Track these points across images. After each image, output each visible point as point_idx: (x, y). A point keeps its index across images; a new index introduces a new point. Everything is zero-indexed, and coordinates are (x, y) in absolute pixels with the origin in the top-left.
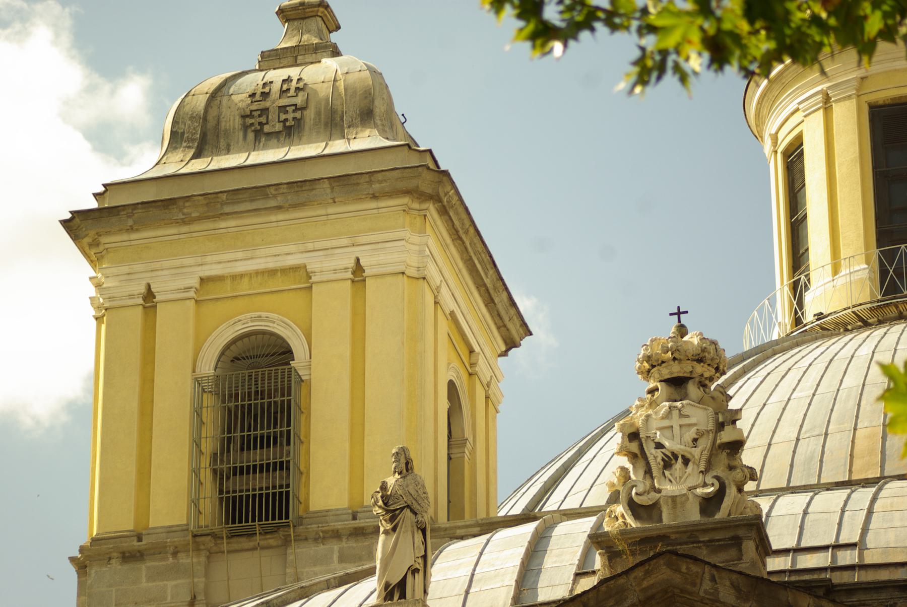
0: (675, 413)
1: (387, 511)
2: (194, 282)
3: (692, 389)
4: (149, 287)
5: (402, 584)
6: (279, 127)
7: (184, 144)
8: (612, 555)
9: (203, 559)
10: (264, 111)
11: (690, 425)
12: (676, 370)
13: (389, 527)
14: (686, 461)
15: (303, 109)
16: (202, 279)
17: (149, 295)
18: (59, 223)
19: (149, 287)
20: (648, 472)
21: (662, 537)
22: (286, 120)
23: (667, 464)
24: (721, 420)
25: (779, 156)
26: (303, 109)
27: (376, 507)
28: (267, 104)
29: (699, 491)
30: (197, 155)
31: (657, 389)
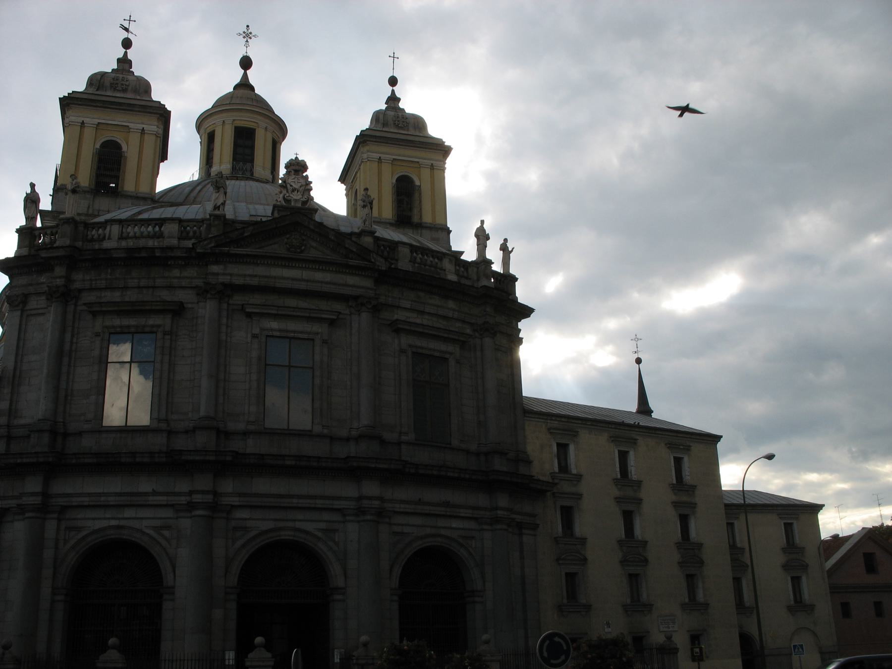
0: (296, 179)
1: (216, 186)
2: (97, 123)
3: (300, 173)
4: (83, 121)
5: (219, 206)
6: (121, 89)
7: (94, 87)
8: (279, 211)
9: (92, 196)
10: (117, 84)
11: (299, 182)
12: (297, 168)
13: (217, 191)
14: (298, 192)
15: (128, 86)
16: (99, 123)
17: (83, 123)
18: (58, 99)
19: (83, 121)
20: (287, 192)
21: (293, 208)
22: (123, 88)
23: (293, 190)
24: (307, 183)
25: (207, 134)
26: (128, 86)
27: (228, 182)
28: (117, 82)
29: (302, 199)
30: (97, 90)
31: (291, 171)
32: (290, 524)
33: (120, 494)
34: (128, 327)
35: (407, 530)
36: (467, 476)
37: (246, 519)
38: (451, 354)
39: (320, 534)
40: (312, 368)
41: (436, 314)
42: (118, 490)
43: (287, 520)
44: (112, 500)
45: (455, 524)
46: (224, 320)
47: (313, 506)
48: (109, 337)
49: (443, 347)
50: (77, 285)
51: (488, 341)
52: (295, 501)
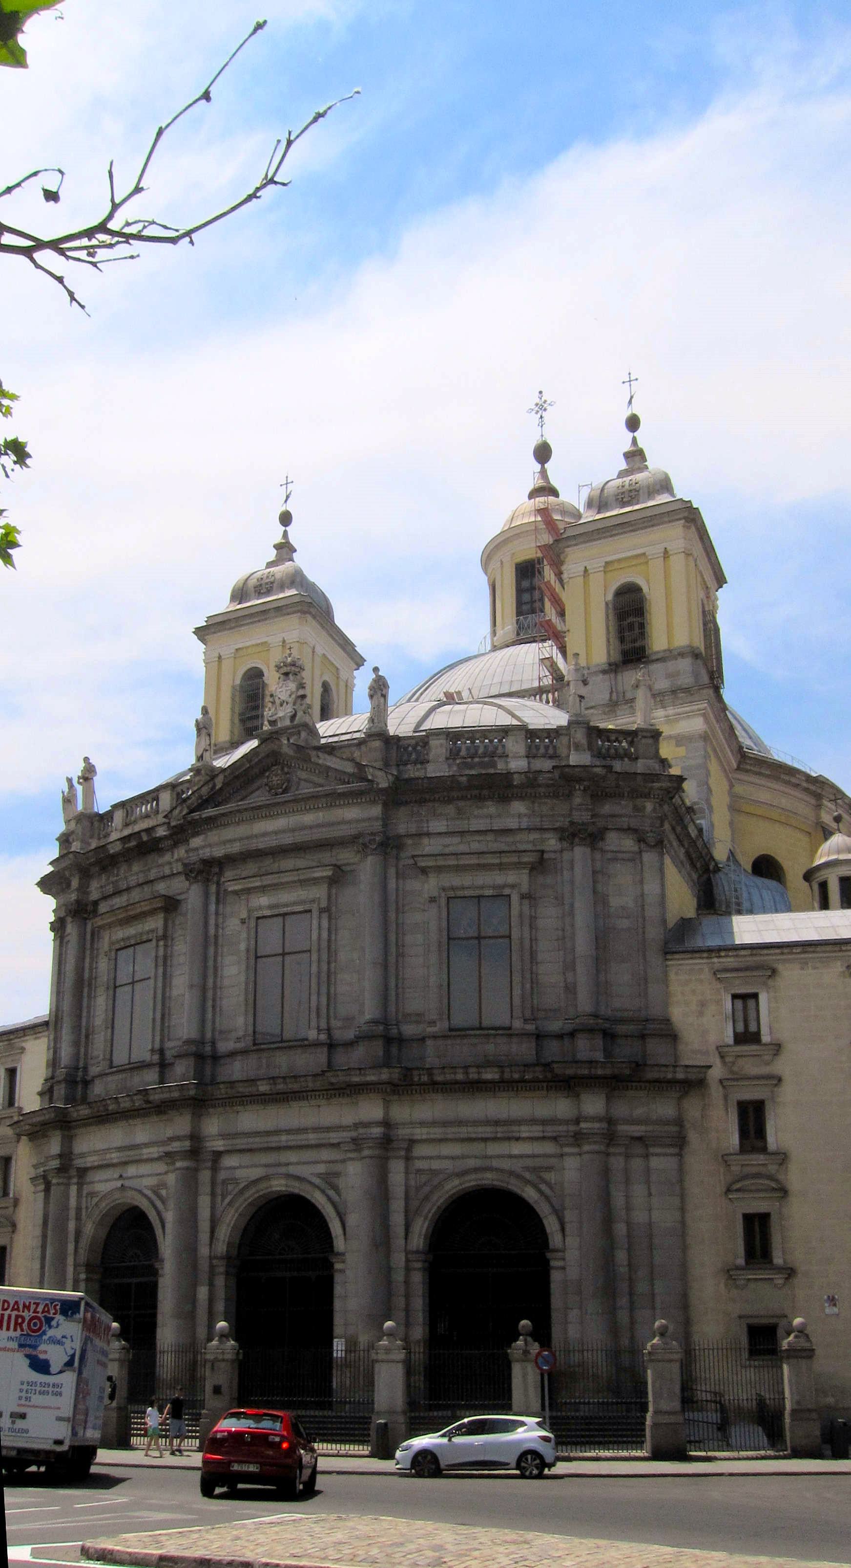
32: (283, 1170)
33: (120, 1149)
34: (128, 938)
35: (436, 1165)
36: (516, 1076)
37: (235, 1168)
38: (513, 886)
39: (317, 1181)
40: (310, 951)
41: (491, 831)
42: (118, 1144)
43: (279, 1165)
44: (115, 1157)
45: (517, 1149)
46: (212, 908)
47: (306, 1143)
48: (116, 954)
49: (499, 878)
50: (94, 895)
51: (580, 853)
52: (284, 1138)
